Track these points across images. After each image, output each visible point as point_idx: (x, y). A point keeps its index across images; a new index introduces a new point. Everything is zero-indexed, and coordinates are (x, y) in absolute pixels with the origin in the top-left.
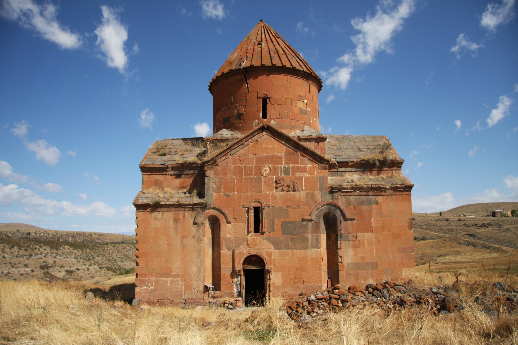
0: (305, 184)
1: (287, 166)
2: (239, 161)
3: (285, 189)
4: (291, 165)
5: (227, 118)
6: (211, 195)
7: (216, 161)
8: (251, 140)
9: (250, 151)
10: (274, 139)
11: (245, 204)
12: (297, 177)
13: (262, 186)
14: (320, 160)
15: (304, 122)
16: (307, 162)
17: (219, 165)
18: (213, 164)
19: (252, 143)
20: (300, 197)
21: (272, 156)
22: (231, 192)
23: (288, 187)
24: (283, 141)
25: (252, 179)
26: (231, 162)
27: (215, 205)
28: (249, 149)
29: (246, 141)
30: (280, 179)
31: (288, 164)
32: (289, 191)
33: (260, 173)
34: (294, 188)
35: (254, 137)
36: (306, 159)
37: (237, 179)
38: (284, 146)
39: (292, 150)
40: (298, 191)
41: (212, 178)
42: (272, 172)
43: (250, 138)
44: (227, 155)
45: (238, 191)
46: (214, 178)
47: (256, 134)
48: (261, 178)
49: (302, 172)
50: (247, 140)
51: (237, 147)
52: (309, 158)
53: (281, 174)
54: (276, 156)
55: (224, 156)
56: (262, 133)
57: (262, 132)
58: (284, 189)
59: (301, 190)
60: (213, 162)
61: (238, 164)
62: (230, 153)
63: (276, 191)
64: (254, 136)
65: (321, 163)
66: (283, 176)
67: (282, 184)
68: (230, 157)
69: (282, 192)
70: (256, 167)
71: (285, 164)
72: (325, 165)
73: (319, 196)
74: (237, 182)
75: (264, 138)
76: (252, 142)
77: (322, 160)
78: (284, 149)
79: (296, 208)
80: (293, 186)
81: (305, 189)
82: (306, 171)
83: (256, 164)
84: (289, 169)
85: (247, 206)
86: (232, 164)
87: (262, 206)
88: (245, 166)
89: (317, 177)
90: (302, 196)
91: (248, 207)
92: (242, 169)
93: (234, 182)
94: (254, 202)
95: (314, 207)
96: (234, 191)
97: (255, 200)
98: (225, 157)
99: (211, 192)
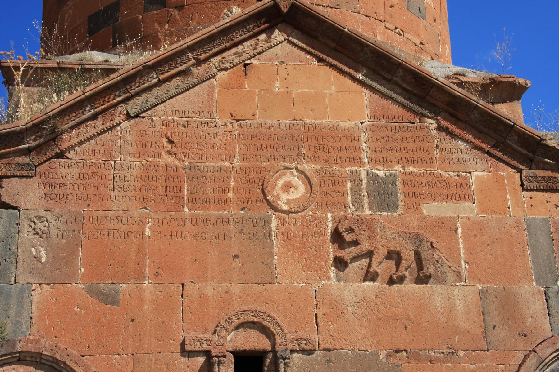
0: (467, 250)
1: (381, 173)
2: (166, 144)
3: (379, 270)
4: (398, 168)
5: (107, 8)
6: (22, 291)
7: (55, 136)
8: (219, 58)
9: (215, 109)
10: (320, 60)
11: (193, 335)
12: (433, 218)
13: (271, 255)
14: (525, 152)
15: (418, 42)
16: (467, 157)
17: (71, 154)
18: (38, 149)
19: (224, 73)
20: (451, 309)
21: (315, 128)
22: (126, 281)
23: (392, 263)
24: (358, 71)
25: (224, 221)
26: (129, 148)
27: (37, 341)
28: (211, 96)
29: (199, 63)
30: (354, 226)
31: (385, 162)
32: (401, 280)
33: (265, 196)
34: (420, 267)
35: (233, 50)
36: (461, 144)
37: (157, 222)
38: (367, 93)
39: (402, 111)
40: (441, 280)
41: (32, 214)
42: (317, 196)
43: (216, 50)
44: (108, 115)
45: (157, 275)
46: (43, 213)
47: (240, 38)
48: (267, 222)
49: (448, 198)
50: (202, 57)
51: (155, 86)
52: (478, 142)
53: (358, 204)
54: (333, 128)
55: (94, 117)
56: (269, 37)
57: (269, 31)
58: (375, 267)
59: (451, 278)
60: (42, 140)
61: (160, 156)
62: (122, 109)
63: (339, 280)
64: (236, 45)
65: (530, 163)
66: (367, 212)
67: (365, 246)
68: (126, 124)
69: (368, 283)
70: (246, 170)
71: (374, 161)
72: (549, 174)
73: (539, 306)
74: (153, 233)
75: (277, 56)
76: (226, 69)
77: (534, 153)
78: (366, 104)
79: (438, 360)
80: (418, 255)
81: (472, 274)
82: (467, 197)
83: (244, 158)
84: (394, 184)
85: (205, 347)
86: (134, 154)
87: (274, 345)
88: (192, 167)
89: (518, 222)
90: (459, 305)
91: (207, 353)
92: (180, 179)
93: (142, 235)
94: (237, 328)
95: (521, 355)
96: (140, 277)
97: (246, 319)
98: (99, 124)
99: (21, 280)
